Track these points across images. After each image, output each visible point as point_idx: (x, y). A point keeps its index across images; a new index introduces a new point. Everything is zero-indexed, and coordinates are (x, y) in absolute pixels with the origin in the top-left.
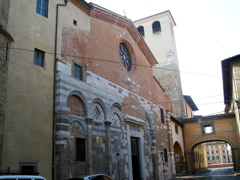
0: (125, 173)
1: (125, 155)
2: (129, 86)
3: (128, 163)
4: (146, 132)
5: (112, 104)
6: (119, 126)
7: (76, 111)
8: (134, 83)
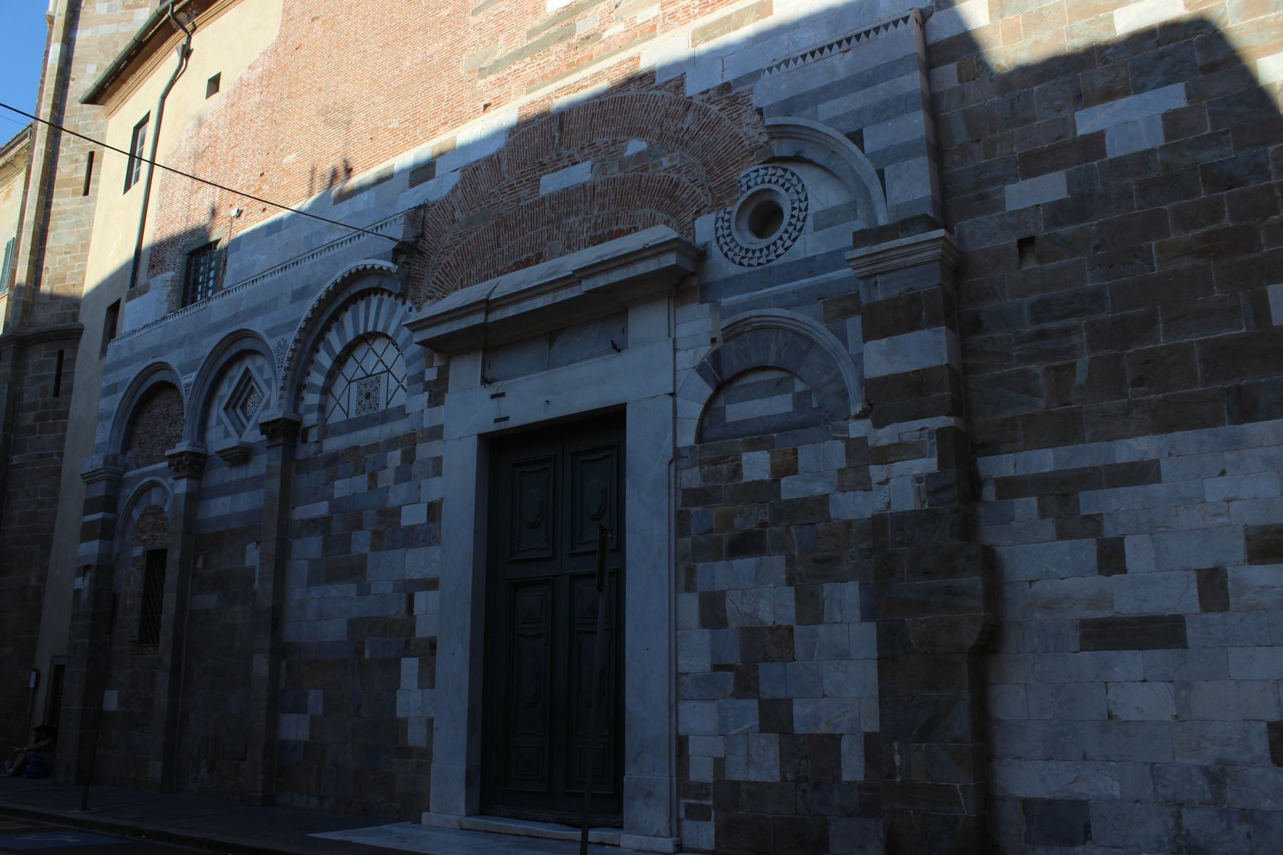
1: (409, 590)
2: (562, 46)
3: (432, 645)
4: (732, 310)
5: (307, 313)
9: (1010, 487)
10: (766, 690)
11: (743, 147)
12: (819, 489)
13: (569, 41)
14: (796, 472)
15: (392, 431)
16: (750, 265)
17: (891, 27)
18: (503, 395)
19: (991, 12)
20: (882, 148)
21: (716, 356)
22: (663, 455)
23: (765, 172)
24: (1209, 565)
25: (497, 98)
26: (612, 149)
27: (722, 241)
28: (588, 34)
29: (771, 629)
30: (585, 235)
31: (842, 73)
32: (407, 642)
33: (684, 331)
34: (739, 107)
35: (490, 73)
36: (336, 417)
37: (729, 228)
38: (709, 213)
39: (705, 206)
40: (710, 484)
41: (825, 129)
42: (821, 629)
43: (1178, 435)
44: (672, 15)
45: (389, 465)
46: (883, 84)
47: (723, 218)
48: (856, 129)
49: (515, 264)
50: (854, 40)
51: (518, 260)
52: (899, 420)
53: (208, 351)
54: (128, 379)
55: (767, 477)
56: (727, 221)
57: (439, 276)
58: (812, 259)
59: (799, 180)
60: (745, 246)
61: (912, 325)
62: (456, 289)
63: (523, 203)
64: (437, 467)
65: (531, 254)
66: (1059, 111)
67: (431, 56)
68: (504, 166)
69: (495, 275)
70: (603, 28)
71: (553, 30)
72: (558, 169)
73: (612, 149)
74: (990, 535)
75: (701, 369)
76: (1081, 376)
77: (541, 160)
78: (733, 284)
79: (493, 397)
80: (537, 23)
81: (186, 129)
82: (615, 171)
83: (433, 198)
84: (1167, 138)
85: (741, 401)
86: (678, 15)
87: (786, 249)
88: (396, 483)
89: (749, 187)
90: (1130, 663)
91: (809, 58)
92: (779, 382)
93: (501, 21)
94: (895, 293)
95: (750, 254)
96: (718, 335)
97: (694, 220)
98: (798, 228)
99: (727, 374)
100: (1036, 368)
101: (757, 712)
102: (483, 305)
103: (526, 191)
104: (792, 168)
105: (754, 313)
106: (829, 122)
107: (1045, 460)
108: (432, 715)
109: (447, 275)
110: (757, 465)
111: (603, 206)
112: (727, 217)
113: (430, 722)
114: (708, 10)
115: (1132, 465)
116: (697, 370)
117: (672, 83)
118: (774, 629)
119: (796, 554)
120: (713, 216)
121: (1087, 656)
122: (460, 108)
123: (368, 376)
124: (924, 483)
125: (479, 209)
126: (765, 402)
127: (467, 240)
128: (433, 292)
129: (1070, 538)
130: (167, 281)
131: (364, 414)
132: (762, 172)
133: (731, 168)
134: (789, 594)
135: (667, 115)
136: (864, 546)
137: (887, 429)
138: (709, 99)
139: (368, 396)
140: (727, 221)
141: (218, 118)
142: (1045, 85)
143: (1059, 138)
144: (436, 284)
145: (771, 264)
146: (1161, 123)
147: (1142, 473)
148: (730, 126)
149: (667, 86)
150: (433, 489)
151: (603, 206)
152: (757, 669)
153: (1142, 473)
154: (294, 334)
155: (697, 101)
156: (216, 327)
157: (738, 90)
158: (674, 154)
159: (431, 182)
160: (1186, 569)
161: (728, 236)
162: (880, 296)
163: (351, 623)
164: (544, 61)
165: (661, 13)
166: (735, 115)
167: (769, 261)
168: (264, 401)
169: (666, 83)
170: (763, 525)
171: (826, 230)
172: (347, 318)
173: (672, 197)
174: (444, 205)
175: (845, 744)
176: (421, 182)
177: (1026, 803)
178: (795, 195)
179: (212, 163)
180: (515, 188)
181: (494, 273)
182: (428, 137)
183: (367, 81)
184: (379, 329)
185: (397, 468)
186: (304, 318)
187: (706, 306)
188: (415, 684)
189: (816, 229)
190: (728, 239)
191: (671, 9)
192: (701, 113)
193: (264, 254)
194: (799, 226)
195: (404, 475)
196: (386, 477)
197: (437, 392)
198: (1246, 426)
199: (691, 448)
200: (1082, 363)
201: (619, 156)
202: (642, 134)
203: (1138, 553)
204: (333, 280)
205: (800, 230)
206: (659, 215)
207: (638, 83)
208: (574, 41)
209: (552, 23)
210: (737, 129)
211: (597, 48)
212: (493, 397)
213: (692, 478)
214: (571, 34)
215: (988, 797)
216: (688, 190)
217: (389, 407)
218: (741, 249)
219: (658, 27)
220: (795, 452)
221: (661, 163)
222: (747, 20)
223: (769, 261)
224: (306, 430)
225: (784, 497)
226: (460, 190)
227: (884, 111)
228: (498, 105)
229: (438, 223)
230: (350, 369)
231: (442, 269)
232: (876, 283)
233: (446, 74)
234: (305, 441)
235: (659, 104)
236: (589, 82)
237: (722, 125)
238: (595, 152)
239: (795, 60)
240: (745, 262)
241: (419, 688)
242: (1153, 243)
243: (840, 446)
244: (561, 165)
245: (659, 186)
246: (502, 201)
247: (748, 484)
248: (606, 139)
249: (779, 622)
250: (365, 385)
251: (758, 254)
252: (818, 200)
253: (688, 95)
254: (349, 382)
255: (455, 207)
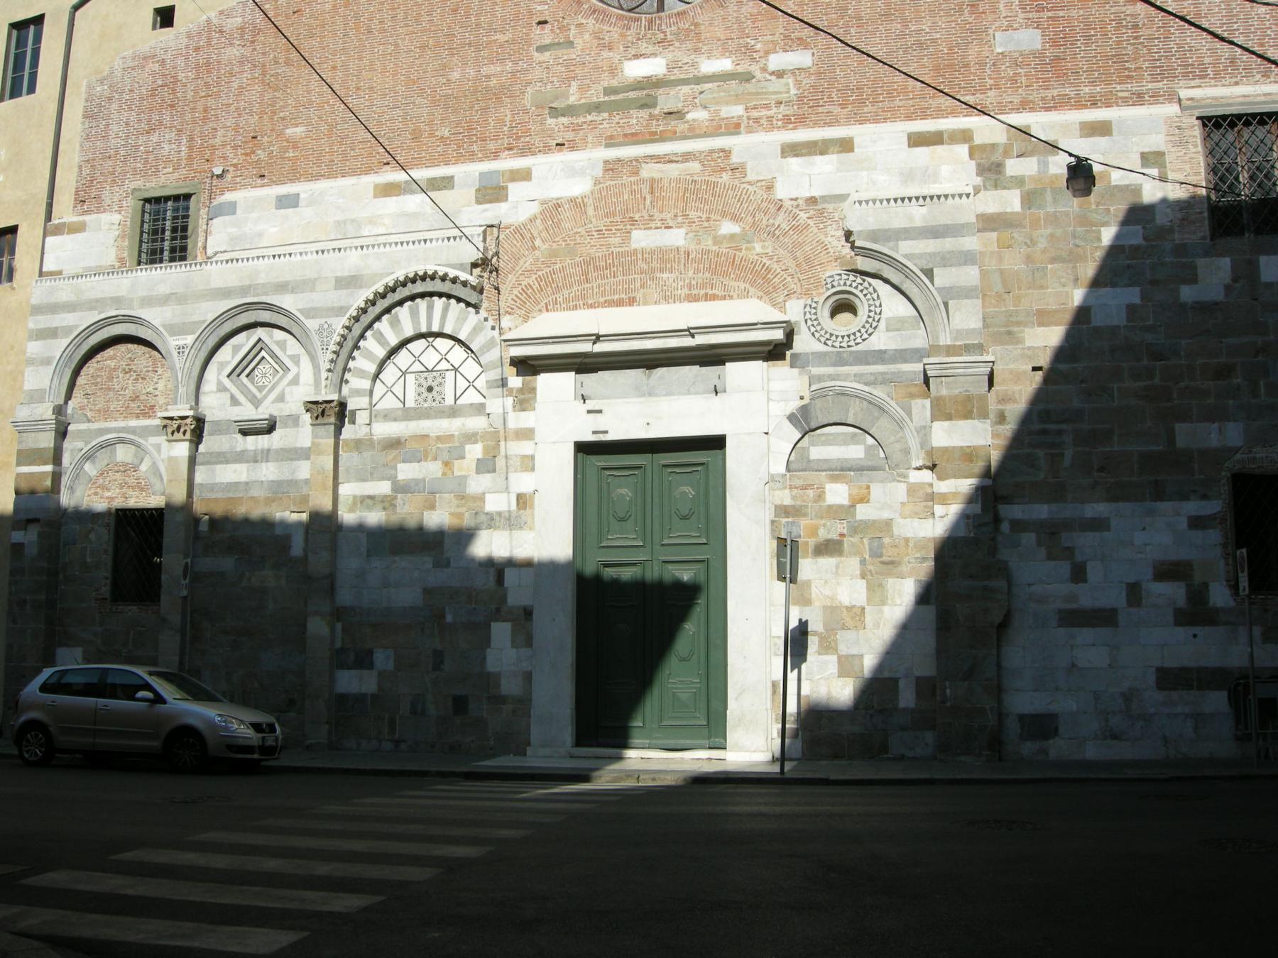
0: (492, 666)
2: (644, 114)
3: (528, 613)
4: (820, 378)
6: (472, 397)
7: (135, 398)
8: (724, 64)
9: (1018, 526)
10: (843, 649)
11: (828, 253)
12: (886, 515)
13: (651, 110)
14: (868, 501)
15: (463, 425)
16: (833, 346)
17: (957, 198)
18: (600, 411)
19: (1022, 203)
20: (947, 286)
21: (804, 410)
22: (760, 479)
23: (847, 277)
24: (1132, 580)
25: (571, 141)
26: (706, 224)
27: (810, 323)
28: (671, 110)
29: (847, 607)
30: (680, 291)
31: (918, 223)
32: (498, 610)
33: (775, 386)
34: (825, 220)
35: (563, 115)
36: (390, 403)
37: (816, 314)
38: (798, 298)
39: (795, 292)
40: (798, 503)
41: (904, 261)
42: (886, 609)
43: (1121, 504)
44: (757, 120)
45: (467, 456)
46: (949, 239)
47: (810, 306)
48: (928, 267)
49: (605, 302)
50: (928, 199)
51: (609, 298)
52: (955, 477)
53: (210, 317)
54: (77, 326)
55: (846, 502)
56: (814, 308)
57: (519, 295)
58: (884, 352)
59: (875, 291)
60: (830, 331)
61: (967, 415)
62: (540, 311)
63: (613, 249)
64: (528, 463)
65: (623, 296)
66: (1064, 286)
67: (487, 77)
68: (590, 211)
69: (585, 307)
70: (686, 110)
71: (632, 95)
72: (651, 228)
73: (706, 224)
74: (1005, 554)
75: (792, 418)
76: (1067, 461)
77: (632, 215)
78: (820, 358)
79: (589, 412)
80: (614, 83)
81: (122, 55)
82: (708, 243)
83: (505, 222)
84: (1128, 321)
85: (822, 445)
86: (762, 121)
87: (864, 340)
88: (478, 471)
89: (833, 286)
90: (1085, 635)
91: (892, 201)
92: (855, 435)
93: (572, 68)
94: (957, 392)
95: (834, 338)
96: (807, 395)
97: (785, 301)
98: (873, 326)
99: (813, 425)
100: (1040, 453)
101: (836, 664)
102: (594, 338)
103: (617, 239)
104: (874, 282)
105: (838, 383)
106: (906, 256)
107: (1042, 511)
108: (529, 669)
109: (530, 297)
110: (837, 494)
111: (697, 271)
112: (814, 305)
113: (528, 677)
114: (791, 126)
115: (1094, 519)
116: (788, 418)
117: (763, 183)
118: (849, 609)
119: (867, 557)
120: (802, 302)
121: (1062, 630)
122: (527, 139)
123: (428, 371)
124: (971, 520)
125: (564, 244)
126: (843, 448)
127: (551, 269)
128: (513, 309)
129: (1054, 560)
130: (113, 224)
131: (426, 405)
132: (844, 277)
133: (818, 267)
134: (862, 584)
135: (759, 209)
136: (918, 555)
137: (947, 482)
138: (798, 206)
139: (430, 389)
140: (814, 308)
141: (175, 57)
142: (1056, 266)
143: (1063, 304)
144: (516, 302)
145: (851, 349)
146: (1125, 310)
147: (1098, 525)
148: (816, 234)
149: (759, 184)
150: (523, 482)
151: (697, 271)
152: (837, 633)
153: (1098, 525)
154: (344, 321)
155: (787, 204)
156: (225, 293)
157: (824, 206)
158: (766, 244)
159: (503, 205)
160: (1121, 582)
161: (815, 320)
162: (944, 392)
163: (427, 592)
164: (624, 121)
165: (746, 115)
166: (821, 226)
167: (849, 346)
168: (290, 376)
169: (758, 181)
170: (842, 535)
171: (896, 333)
172: (403, 312)
173: (765, 277)
174: (519, 231)
175: (902, 684)
176: (491, 202)
177: (1022, 718)
178: (871, 302)
179: (172, 106)
180: (604, 234)
181: (584, 304)
182: (488, 157)
183: (403, 78)
184: (435, 329)
185: (478, 460)
186: (355, 306)
187: (796, 371)
188: (509, 644)
189: (888, 330)
190: (815, 323)
191: (755, 114)
192: (791, 215)
193: (275, 226)
194: (874, 324)
195: (486, 465)
196: (465, 466)
197: (525, 400)
198: (1158, 504)
199: (784, 476)
200: (1069, 453)
201: (712, 232)
202: (735, 218)
203: (1094, 572)
204: (394, 277)
205: (875, 328)
206: (752, 290)
207: (730, 173)
208: (656, 111)
209: (631, 88)
210: (822, 237)
211: (681, 127)
212: (589, 412)
213: (785, 498)
214: (654, 105)
215: (1001, 716)
216: (779, 276)
217: (457, 402)
218: (826, 332)
219: (742, 126)
220: (868, 487)
221: (754, 249)
222: (832, 149)
223: (849, 346)
224: (353, 412)
225: (858, 518)
226: (538, 221)
227: (947, 260)
228: (573, 149)
229: (515, 245)
230: (403, 358)
231: (522, 289)
232: (942, 382)
233: (508, 100)
234: (353, 422)
235: (751, 197)
236: (680, 159)
237: (810, 230)
238: (689, 223)
239: (881, 201)
240: (829, 343)
241: (513, 647)
242: (1115, 386)
243: (902, 488)
244: (653, 226)
245: (752, 266)
246: (589, 243)
247: (830, 507)
248: (699, 214)
249: (854, 603)
250: (426, 378)
251: (840, 339)
252: (890, 309)
253: (779, 198)
254: (404, 373)
255: (535, 235)
